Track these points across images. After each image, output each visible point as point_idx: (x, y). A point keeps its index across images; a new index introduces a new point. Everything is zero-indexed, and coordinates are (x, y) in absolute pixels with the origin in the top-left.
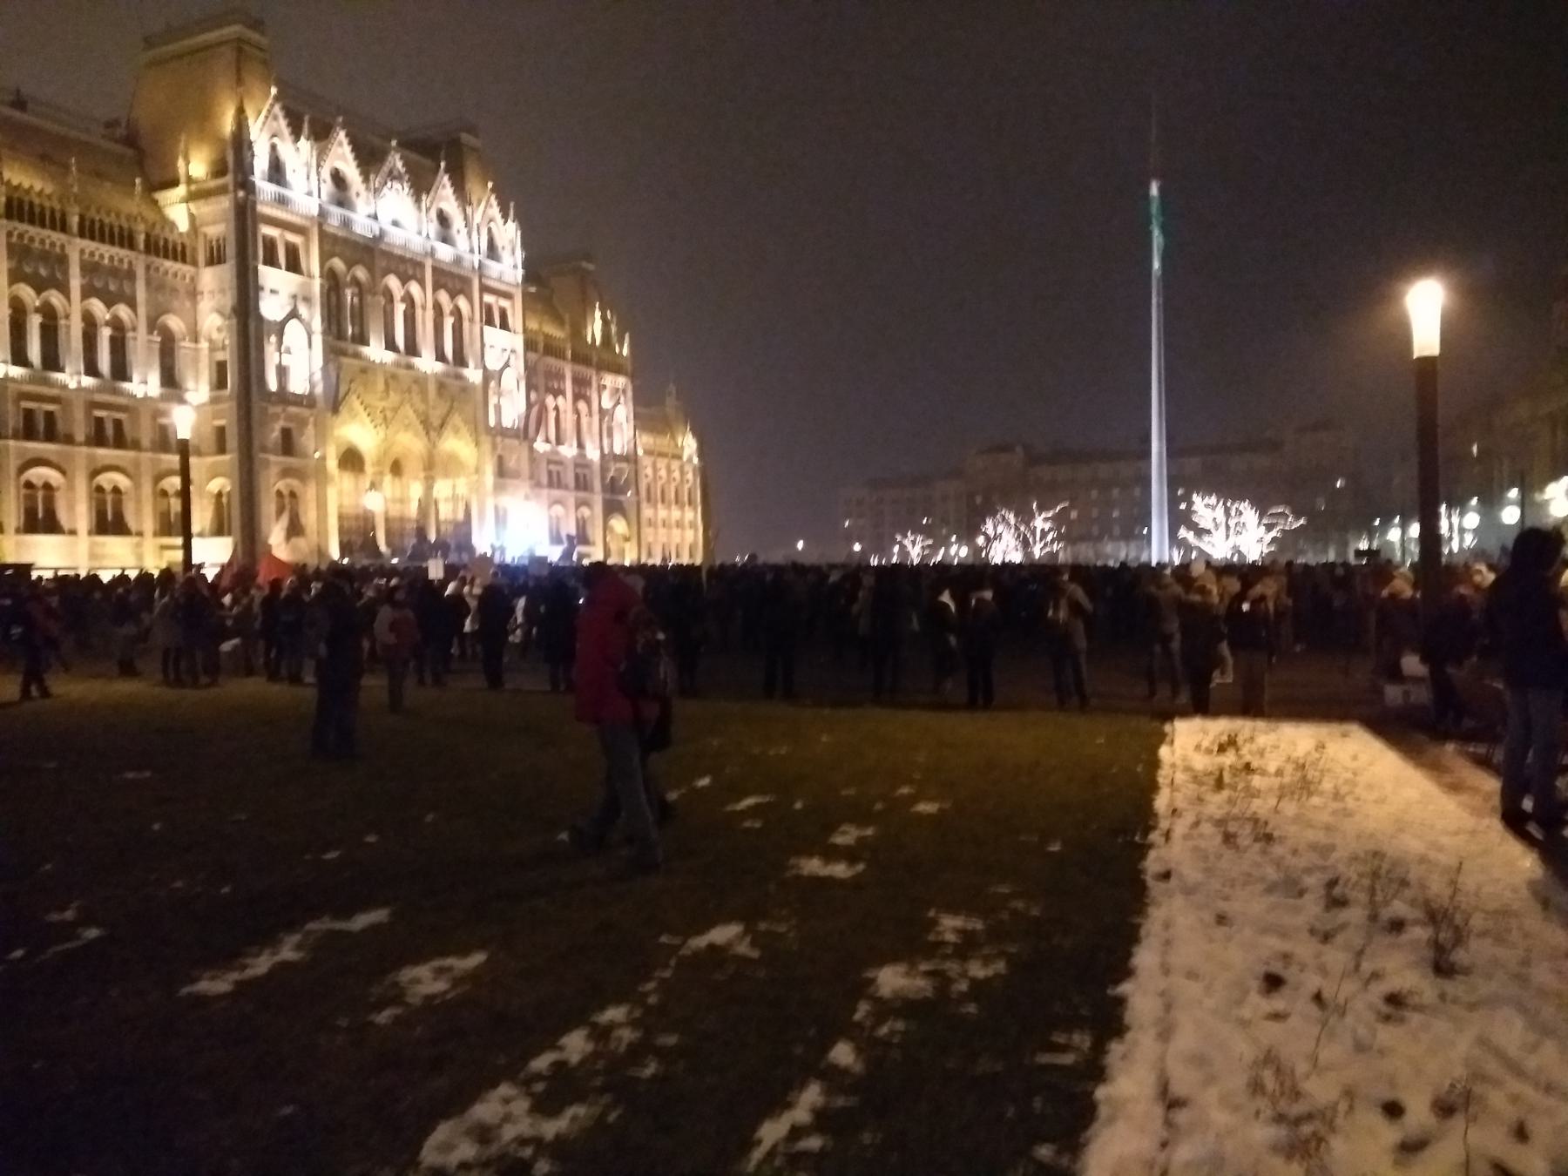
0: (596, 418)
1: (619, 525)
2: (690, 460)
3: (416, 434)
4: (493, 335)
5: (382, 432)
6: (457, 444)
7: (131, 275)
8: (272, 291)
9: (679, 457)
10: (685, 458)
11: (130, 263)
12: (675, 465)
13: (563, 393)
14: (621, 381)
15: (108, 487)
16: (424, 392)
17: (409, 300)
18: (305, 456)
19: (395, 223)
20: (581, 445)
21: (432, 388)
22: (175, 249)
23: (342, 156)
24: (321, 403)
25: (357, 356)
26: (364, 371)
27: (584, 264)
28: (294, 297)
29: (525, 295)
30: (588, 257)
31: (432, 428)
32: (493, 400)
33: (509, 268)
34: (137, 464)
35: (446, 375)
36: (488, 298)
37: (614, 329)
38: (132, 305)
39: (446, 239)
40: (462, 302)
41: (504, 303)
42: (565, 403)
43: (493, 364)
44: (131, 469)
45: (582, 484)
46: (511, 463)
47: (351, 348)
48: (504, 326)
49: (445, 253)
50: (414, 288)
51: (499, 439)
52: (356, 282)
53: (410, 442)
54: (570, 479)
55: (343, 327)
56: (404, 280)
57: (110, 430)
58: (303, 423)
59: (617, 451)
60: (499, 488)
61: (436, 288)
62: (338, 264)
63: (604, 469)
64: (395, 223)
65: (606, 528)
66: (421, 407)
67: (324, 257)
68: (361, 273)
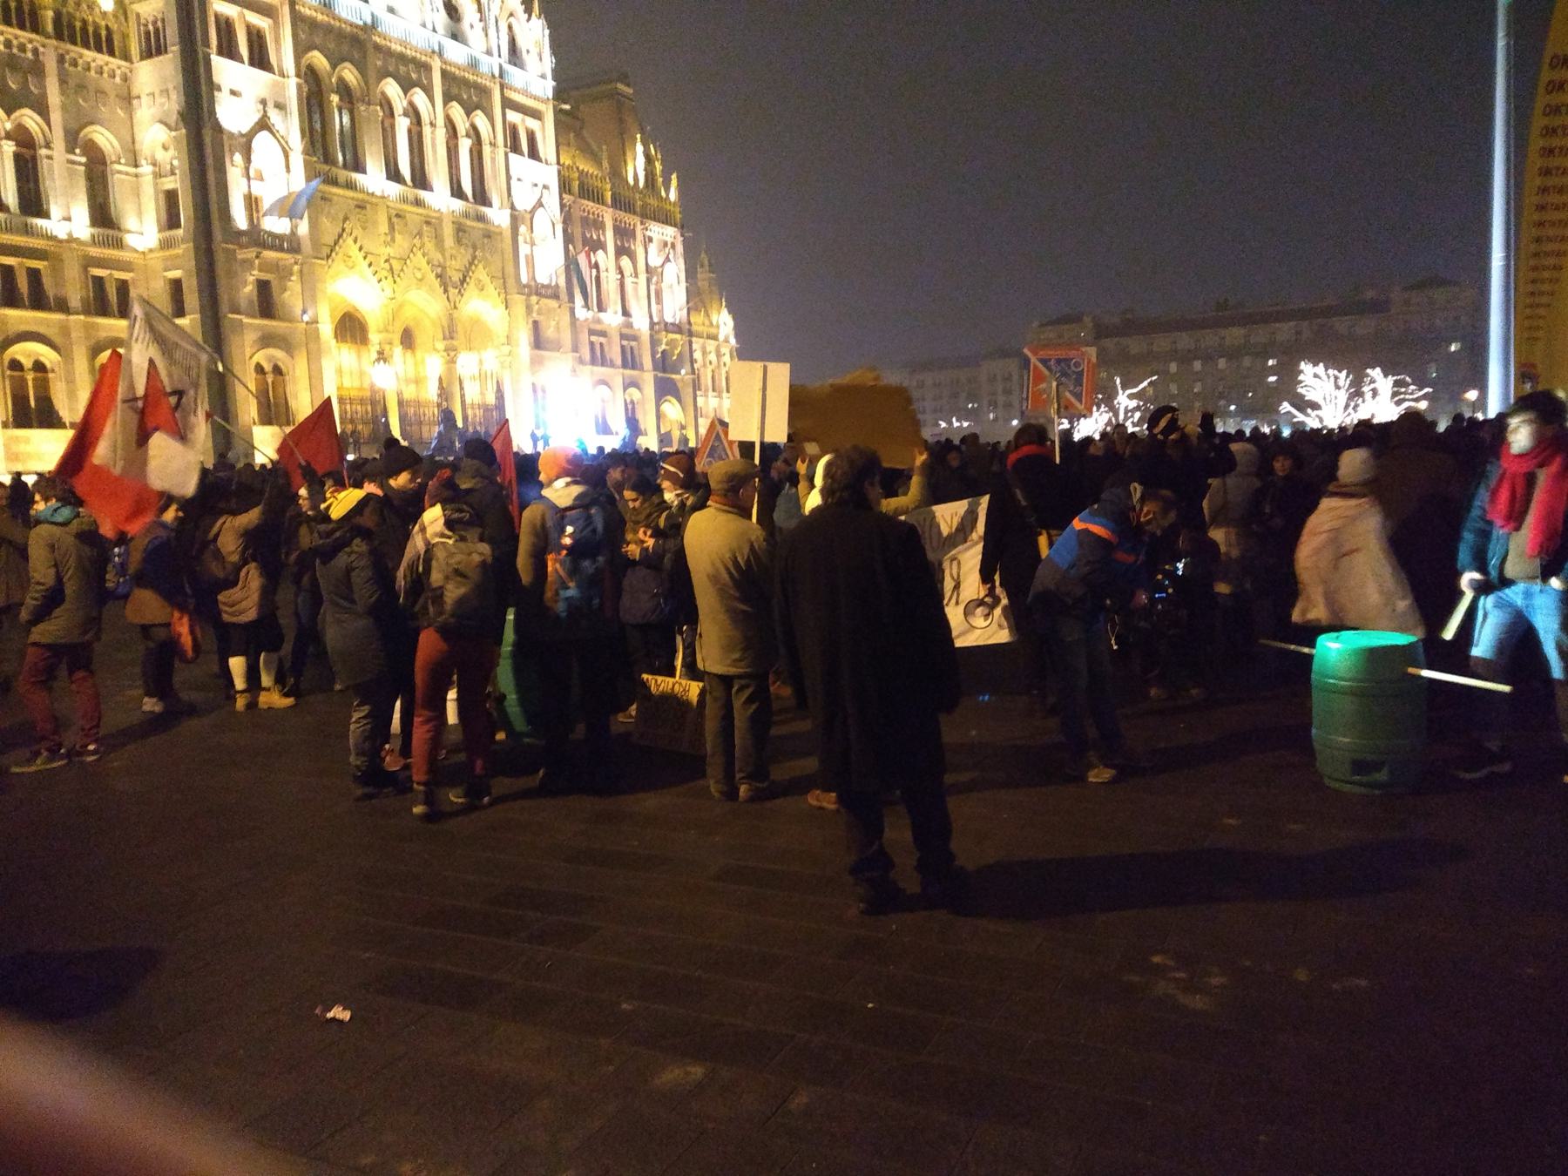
0: (643, 277)
1: (672, 409)
2: (726, 341)
3: (431, 289)
4: (519, 163)
5: (387, 284)
6: (482, 304)
7: (37, 69)
8: (233, 93)
9: (715, 338)
10: (721, 338)
11: (35, 51)
12: (711, 345)
14: (670, 233)
15: (27, 363)
16: (439, 239)
17: (413, 113)
18: (289, 319)
19: (391, 10)
21: (448, 231)
22: (97, 35)
24: (307, 246)
25: (350, 185)
26: (361, 206)
27: (620, 86)
28: (264, 102)
29: (558, 112)
30: (624, 78)
31: (451, 284)
32: (524, 249)
33: (536, 78)
34: (65, 330)
35: (466, 215)
36: (513, 117)
37: (658, 166)
38: (42, 110)
39: (456, 36)
40: (480, 119)
41: (532, 123)
42: (605, 259)
44: (57, 340)
45: (630, 361)
46: (549, 332)
47: (343, 175)
48: (534, 154)
49: (456, 54)
50: (419, 97)
51: (534, 299)
52: (344, 90)
53: (425, 304)
54: (615, 354)
55: (330, 152)
56: (407, 86)
57: (23, 284)
58: (284, 273)
59: (669, 319)
60: (536, 363)
61: (448, 98)
62: (318, 59)
63: (654, 343)
64: (391, 10)
65: (659, 416)
66: (437, 257)
67: (300, 50)
68: (349, 74)
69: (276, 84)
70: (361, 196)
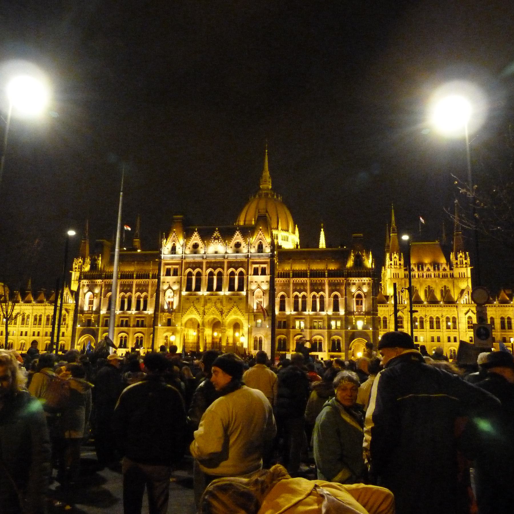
7: (148, 285)
13: (324, 291)
20: (336, 308)
23: (196, 238)
25: (195, 295)
42: (326, 295)
43: (253, 287)
44: (144, 333)
57: (140, 323)
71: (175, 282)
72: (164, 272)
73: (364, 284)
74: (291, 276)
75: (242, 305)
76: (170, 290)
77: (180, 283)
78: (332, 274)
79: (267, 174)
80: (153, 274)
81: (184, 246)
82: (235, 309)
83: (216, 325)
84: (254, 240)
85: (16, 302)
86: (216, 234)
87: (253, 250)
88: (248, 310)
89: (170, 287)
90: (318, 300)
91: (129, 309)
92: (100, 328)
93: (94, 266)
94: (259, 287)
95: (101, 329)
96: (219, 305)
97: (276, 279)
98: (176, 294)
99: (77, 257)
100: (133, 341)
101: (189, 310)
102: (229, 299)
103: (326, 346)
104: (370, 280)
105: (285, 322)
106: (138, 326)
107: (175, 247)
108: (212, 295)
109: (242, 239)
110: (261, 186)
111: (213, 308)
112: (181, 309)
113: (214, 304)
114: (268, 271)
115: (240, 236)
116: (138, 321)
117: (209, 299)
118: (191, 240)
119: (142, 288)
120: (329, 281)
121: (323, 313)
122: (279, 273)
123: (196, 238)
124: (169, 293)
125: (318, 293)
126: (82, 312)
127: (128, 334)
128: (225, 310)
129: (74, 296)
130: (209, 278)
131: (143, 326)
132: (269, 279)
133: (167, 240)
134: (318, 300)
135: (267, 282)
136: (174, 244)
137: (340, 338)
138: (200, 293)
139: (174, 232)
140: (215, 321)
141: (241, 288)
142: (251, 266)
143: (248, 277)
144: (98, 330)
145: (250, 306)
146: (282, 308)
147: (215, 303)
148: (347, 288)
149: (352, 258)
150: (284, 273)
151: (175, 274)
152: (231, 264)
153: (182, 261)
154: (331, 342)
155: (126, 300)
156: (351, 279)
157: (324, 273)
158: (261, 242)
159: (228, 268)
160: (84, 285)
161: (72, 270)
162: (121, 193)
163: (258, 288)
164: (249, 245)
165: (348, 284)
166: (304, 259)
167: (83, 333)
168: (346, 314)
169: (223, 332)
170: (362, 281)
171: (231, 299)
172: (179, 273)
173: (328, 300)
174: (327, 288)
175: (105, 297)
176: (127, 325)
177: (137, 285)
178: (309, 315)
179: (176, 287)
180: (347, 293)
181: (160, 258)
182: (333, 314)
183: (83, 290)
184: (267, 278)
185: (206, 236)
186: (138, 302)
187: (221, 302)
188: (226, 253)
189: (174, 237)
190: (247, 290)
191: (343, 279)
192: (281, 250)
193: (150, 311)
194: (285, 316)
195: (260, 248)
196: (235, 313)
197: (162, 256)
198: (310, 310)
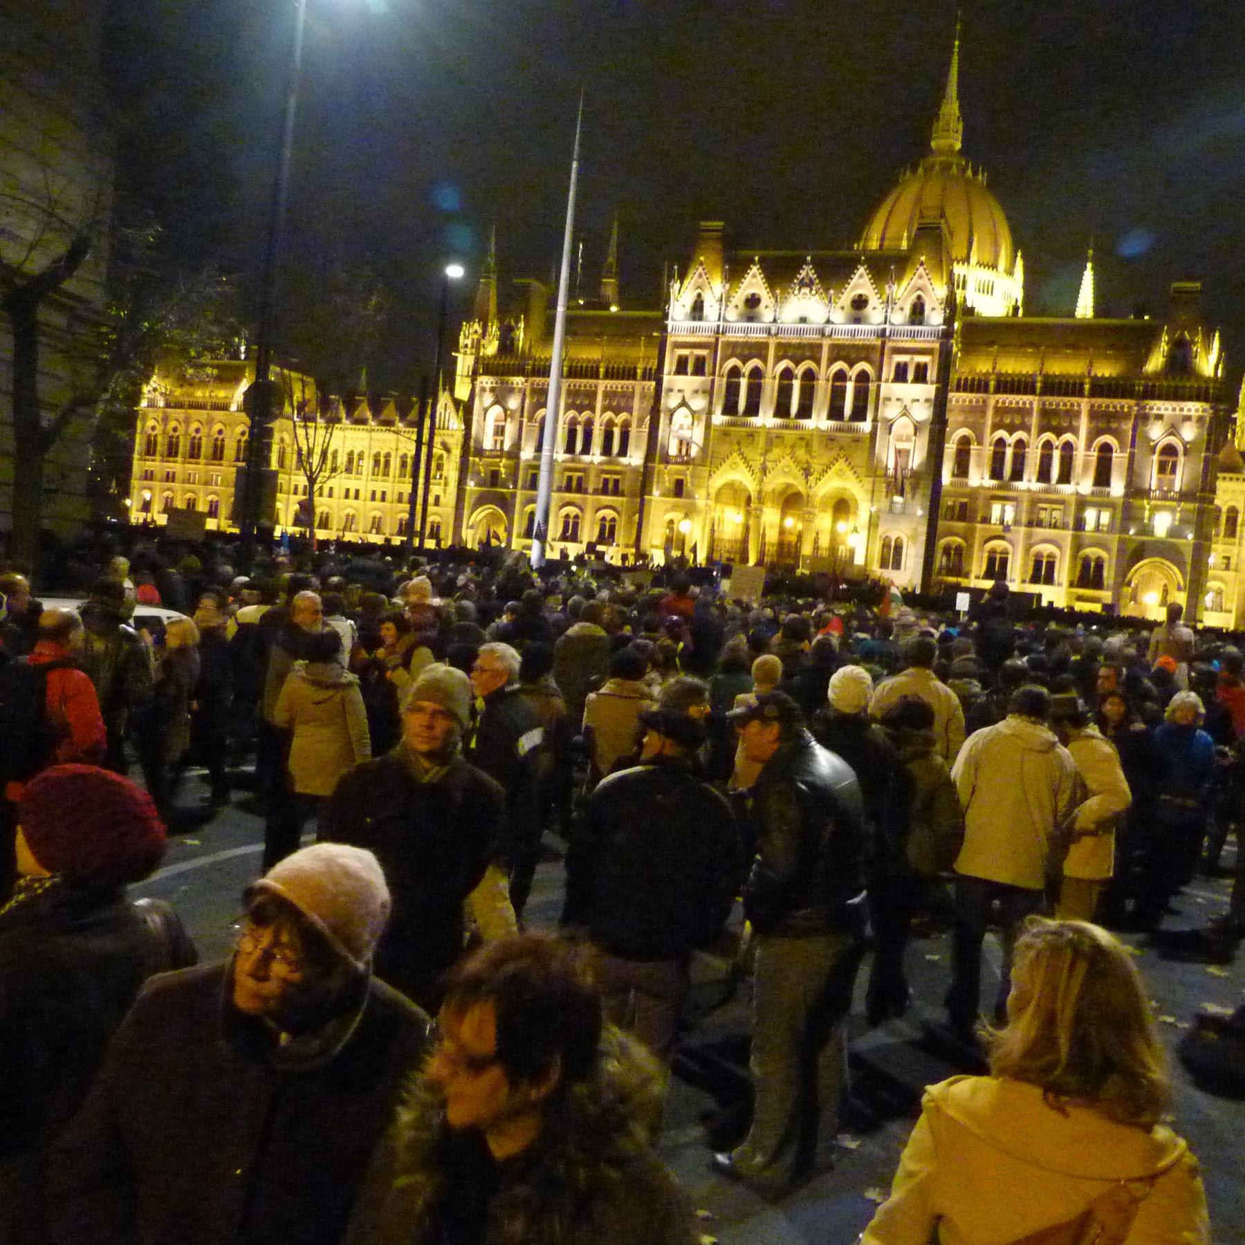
7: (632, 396)
13: (1075, 431)
20: (1103, 478)
23: (754, 282)
25: (745, 425)
42: (1080, 442)
44: (619, 508)
57: (611, 486)
69: (704, 382)
70: (747, 429)
71: (696, 392)
72: (671, 365)
73: (1188, 418)
74: (992, 388)
75: (861, 457)
76: (684, 409)
77: (709, 392)
78: (1102, 388)
79: (951, 108)
80: (645, 369)
81: (725, 300)
82: (841, 464)
83: (791, 501)
84: (903, 291)
85: (333, 421)
86: (807, 272)
87: (899, 318)
88: (873, 469)
89: (684, 404)
90: (1057, 455)
91: (586, 450)
92: (519, 493)
93: (507, 345)
94: (905, 412)
95: (520, 495)
96: (801, 453)
97: (951, 395)
98: (699, 420)
99: (469, 319)
100: (592, 528)
101: (728, 462)
102: (829, 439)
103: (1063, 572)
104: (1204, 410)
105: (963, 506)
106: (605, 491)
107: (703, 303)
108: (787, 427)
109: (871, 287)
110: (933, 144)
111: (787, 461)
112: (709, 458)
113: (788, 451)
114: (932, 374)
115: (866, 278)
116: (606, 481)
117: (778, 437)
118: (743, 286)
119: (618, 403)
120: (1092, 406)
121: (1067, 489)
122: (959, 380)
123: (754, 282)
124: (682, 417)
125: (1058, 435)
126: (480, 452)
127: (581, 509)
128: (816, 467)
129: (461, 414)
130: (780, 385)
131: (616, 492)
132: (932, 395)
133: (682, 283)
134: (1057, 455)
135: (927, 400)
136: (699, 295)
137: (1104, 554)
138: (756, 421)
139: (701, 264)
140: (789, 492)
141: (859, 414)
142: (890, 358)
143: (879, 387)
144: (514, 495)
145: (880, 461)
146: (962, 470)
147: (793, 447)
148: (1140, 428)
149: (1164, 347)
150: (973, 380)
151: (699, 370)
152: (839, 352)
153: (717, 339)
154: (1079, 563)
155: (580, 429)
156: (1151, 403)
157: (1082, 384)
158: (919, 297)
159: (831, 361)
160: (483, 390)
161: (457, 351)
162: (575, 165)
163: (904, 415)
164: (889, 302)
165: (1143, 418)
166: (1031, 344)
167: (481, 501)
168: (1127, 495)
169: (808, 519)
170: (1182, 410)
171: (831, 439)
172: (708, 368)
173: (1084, 456)
174: (1084, 424)
175: (530, 419)
176: (580, 489)
177: (607, 395)
178: (1029, 491)
179: (699, 403)
180: (1137, 440)
181: (664, 329)
182: (1093, 494)
183: (481, 401)
184: (928, 390)
185: (781, 275)
186: (608, 436)
187: (808, 445)
188: (828, 322)
189: (700, 276)
190: (875, 420)
191: (1132, 402)
192: (970, 319)
193: (635, 458)
194: (967, 490)
195: (918, 312)
196: (840, 474)
197: (670, 323)
198: (1034, 478)
